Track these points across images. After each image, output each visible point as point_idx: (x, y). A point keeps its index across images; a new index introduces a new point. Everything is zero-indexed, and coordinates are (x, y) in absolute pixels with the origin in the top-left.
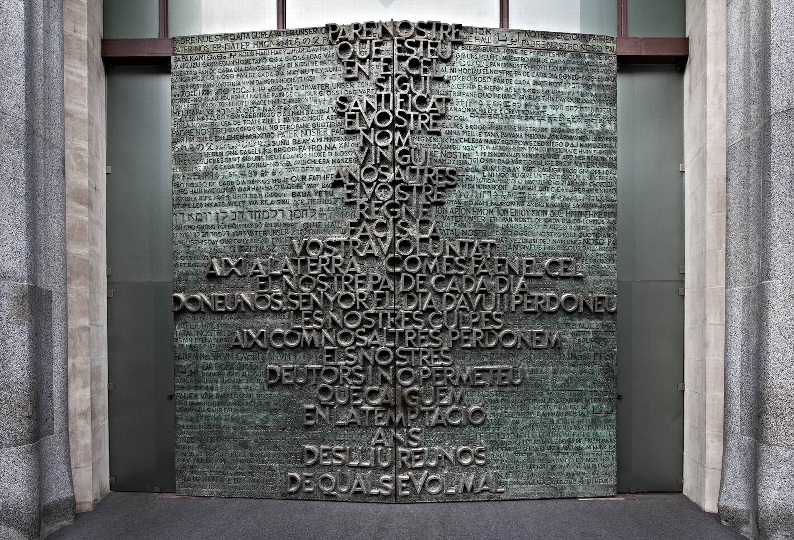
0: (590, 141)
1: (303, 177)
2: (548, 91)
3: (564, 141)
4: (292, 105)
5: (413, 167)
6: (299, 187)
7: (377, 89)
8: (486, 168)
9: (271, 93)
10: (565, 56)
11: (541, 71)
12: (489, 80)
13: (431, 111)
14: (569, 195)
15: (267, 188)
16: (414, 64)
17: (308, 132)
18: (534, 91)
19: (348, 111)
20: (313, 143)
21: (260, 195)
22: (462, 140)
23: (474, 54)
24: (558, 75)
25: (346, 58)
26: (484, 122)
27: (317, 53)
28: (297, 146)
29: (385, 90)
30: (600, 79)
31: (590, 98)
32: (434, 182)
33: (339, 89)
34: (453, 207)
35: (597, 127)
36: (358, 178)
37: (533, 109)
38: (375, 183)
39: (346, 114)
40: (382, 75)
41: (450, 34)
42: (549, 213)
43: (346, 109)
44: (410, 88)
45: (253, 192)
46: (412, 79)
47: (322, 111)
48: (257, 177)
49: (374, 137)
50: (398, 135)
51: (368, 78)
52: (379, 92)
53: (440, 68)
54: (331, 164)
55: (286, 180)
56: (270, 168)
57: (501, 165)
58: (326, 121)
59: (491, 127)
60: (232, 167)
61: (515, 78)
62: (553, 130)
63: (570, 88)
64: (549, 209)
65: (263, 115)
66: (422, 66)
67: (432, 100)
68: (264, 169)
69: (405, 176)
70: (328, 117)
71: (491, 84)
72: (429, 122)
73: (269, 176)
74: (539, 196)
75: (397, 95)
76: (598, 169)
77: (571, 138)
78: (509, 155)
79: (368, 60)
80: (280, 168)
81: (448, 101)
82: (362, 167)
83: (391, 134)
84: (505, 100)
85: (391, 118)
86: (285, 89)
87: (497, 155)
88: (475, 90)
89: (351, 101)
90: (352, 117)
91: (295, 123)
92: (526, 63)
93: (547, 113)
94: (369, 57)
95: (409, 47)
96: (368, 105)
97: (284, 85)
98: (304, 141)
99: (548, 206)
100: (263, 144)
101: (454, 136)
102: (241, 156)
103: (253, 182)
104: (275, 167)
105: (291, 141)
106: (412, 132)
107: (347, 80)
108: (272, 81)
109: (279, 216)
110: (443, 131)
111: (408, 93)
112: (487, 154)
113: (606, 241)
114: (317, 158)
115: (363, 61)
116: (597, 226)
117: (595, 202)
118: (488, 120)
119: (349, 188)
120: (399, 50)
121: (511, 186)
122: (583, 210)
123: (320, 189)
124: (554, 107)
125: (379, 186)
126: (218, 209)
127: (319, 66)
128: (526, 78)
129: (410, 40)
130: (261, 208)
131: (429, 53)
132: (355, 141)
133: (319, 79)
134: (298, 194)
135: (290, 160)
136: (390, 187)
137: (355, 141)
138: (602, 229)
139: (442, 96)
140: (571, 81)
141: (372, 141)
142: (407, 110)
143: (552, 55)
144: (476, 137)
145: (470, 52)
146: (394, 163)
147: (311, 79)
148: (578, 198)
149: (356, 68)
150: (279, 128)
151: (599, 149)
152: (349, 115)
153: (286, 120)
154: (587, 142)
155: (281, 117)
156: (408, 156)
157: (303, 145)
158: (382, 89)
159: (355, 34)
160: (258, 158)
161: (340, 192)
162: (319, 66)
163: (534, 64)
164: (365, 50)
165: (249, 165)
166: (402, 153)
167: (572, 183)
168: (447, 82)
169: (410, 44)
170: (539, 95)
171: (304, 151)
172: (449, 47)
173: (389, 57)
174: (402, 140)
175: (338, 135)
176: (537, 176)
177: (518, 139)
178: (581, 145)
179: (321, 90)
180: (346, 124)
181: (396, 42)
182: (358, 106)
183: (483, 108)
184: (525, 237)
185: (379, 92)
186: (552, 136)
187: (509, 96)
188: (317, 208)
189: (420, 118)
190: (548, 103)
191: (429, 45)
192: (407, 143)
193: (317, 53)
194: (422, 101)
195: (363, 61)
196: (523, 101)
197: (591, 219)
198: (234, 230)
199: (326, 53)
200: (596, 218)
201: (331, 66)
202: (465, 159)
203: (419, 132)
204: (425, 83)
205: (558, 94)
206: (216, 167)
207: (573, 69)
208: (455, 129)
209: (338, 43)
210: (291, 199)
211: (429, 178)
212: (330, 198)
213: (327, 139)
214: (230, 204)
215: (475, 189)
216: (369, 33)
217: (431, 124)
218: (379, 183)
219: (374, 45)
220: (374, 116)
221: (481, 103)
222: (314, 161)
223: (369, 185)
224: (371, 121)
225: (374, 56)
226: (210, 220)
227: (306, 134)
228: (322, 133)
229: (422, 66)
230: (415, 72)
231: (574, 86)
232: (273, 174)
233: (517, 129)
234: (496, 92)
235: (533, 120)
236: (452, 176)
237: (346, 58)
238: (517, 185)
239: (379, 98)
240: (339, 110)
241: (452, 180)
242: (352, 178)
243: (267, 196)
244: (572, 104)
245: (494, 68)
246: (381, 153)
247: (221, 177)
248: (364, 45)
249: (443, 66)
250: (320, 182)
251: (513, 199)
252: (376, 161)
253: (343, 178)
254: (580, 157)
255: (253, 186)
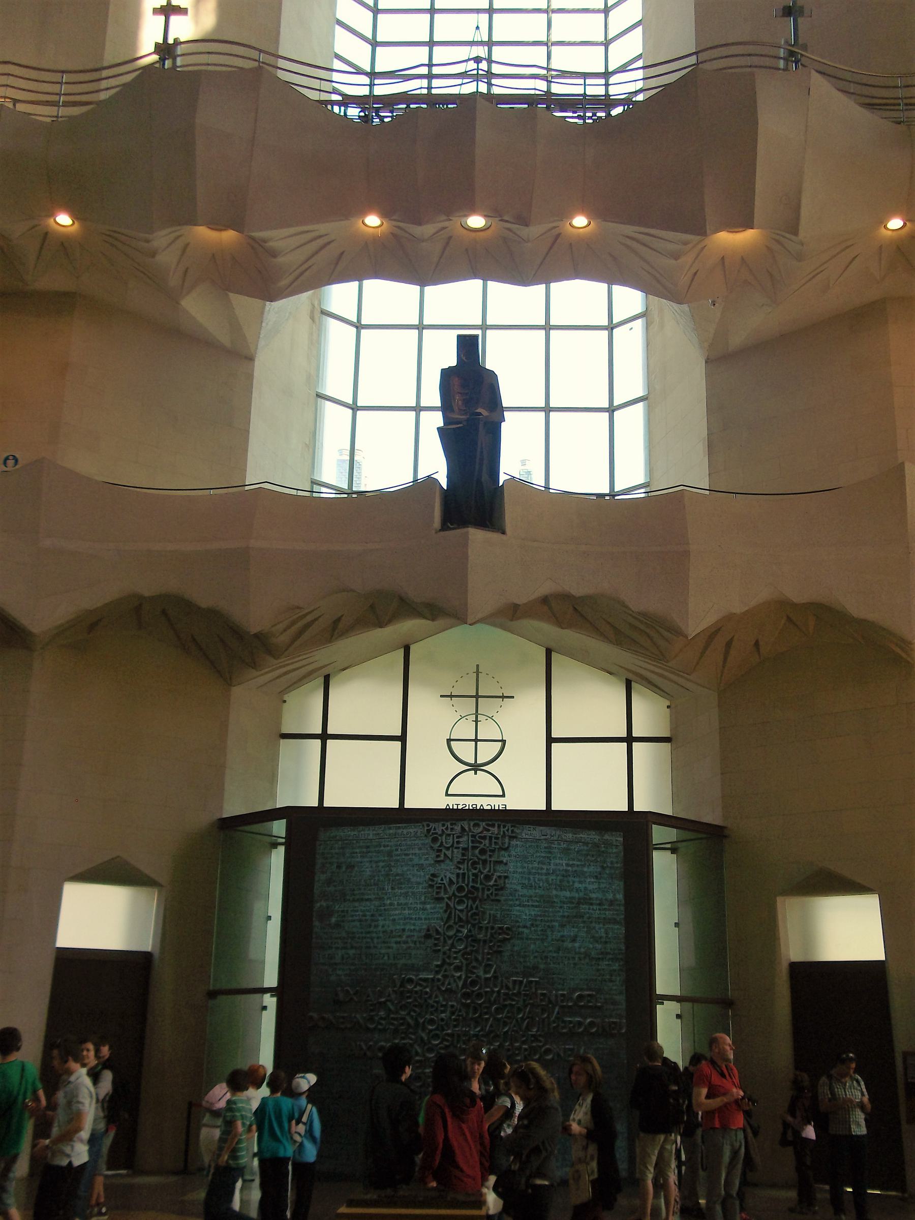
0: (606, 907)
1: (404, 930)
2: (576, 871)
3: (587, 907)
4: (397, 878)
5: (481, 925)
6: (400, 936)
7: (457, 869)
8: (532, 925)
9: (383, 870)
10: (587, 846)
11: (571, 856)
12: (535, 863)
13: (494, 885)
14: (591, 946)
15: (378, 938)
16: (483, 852)
17: (408, 898)
18: (566, 871)
19: (436, 884)
20: (411, 906)
21: (373, 943)
22: (515, 905)
23: (524, 845)
24: (583, 860)
25: (436, 846)
26: (531, 892)
27: (416, 842)
28: (400, 907)
29: (462, 870)
30: (612, 863)
31: (605, 876)
32: (495, 936)
33: (430, 868)
34: (509, 954)
35: (610, 896)
36: (442, 934)
37: (565, 883)
38: (454, 936)
39: (435, 886)
40: (461, 859)
41: (508, 830)
42: (577, 959)
43: (435, 882)
44: (480, 869)
45: (369, 940)
46: (481, 863)
47: (419, 883)
48: (372, 929)
49: (454, 903)
50: (470, 902)
51: (451, 860)
52: (458, 871)
53: (501, 855)
54: (423, 921)
55: (392, 931)
56: (381, 923)
57: (543, 924)
58: (421, 890)
59: (536, 897)
60: (354, 921)
61: (552, 861)
62: (579, 899)
63: (592, 869)
64: (577, 956)
65: (378, 885)
66: (489, 853)
67: (495, 877)
68: (376, 923)
69: (475, 932)
70: (422, 888)
71: (536, 865)
72: (492, 892)
73: (380, 928)
74: (570, 945)
75: (470, 873)
76: (611, 926)
77: (592, 904)
78: (549, 916)
79: (451, 849)
80: (387, 922)
81: (506, 877)
82: (444, 925)
83: (466, 902)
84: (546, 877)
85: (466, 890)
86: (393, 866)
87: (540, 916)
88: (525, 870)
89: (439, 876)
90: (439, 888)
91: (399, 891)
92: (560, 851)
93: (575, 886)
94: (452, 846)
95: (479, 840)
96: (450, 879)
97: (393, 864)
98: (406, 904)
99: (576, 953)
100: (376, 905)
101: (511, 902)
102: (361, 913)
103: (369, 933)
104: (384, 922)
105: (396, 903)
106: (480, 900)
107: (436, 861)
108: (383, 861)
109: (386, 958)
110: (503, 898)
111: (478, 872)
112: (533, 915)
113: (618, 979)
114: (414, 917)
115: (448, 849)
116: (611, 968)
117: (609, 950)
118: (534, 891)
119: (436, 939)
120: (473, 842)
121: (550, 939)
122: (600, 956)
123: (415, 939)
124: (580, 882)
125: (457, 938)
126: (343, 951)
127: (417, 851)
128: (561, 862)
129: (480, 835)
130: (373, 951)
131: (493, 843)
132: (441, 905)
133: (416, 860)
134: (399, 943)
135: (395, 917)
136: (464, 939)
137: (441, 905)
138: (615, 971)
139: (502, 874)
140: (592, 864)
141: (452, 905)
142: (477, 884)
143: (578, 845)
144: (525, 903)
145: (522, 843)
146: (468, 922)
147: (411, 860)
148: (597, 948)
149: (443, 853)
150: (388, 894)
151: (612, 912)
152: (436, 887)
153: (393, 888)
154: (604, 907)
155: (390, 887)
156: (477, 917)
157: (405, 906)
158: (460, 869)
159: (442, 829)
160: (372, 915)
161: (430, 942)
162: (417, 851)
163: (566, 851)
164: (450, 841)
165: (366, 920)
166: (475, 914)
167: (593, 937)
168: (506, 864)
169: (479, 837)
170: (570, 873)
171: (405, 912)
172: (507, 840)
173: (466, 846)
174: (473, 905)
175: (429, 901)
176: (569, 931)
177: (556, 905)
178: (599, 910)
179: (417, 868)
180: (435, 894)
181: (470, 836)
182: (443, 881)
183: (530, 882)
184: (560, 976)
185: (458, 871)
186: (579, 903)
187: (549, 874)
188: (414, 952)
189: (486, 890)
190: (577, 879)
191: (493, 839)
192: (477, 908)
193: (416, 842)
194: (488, 878)
195: (448, 849)
196: (559, 878)
197: (607, 963)
198: (353, 968)
199: (422, 842)
200: (610, 963)
201: (426, 851)
202: (517, 919)
203: (485, 900)
204: (490, 865)
205: (583, 873)
206: (343, 921)
207: (593, 856)
208: (510, 897)
209: (431, 836)
210: (394, 945)
211: (491, 933)
212: (422, 946)
213: (421, 903)
214: (352, 947)
215: (524, 941)
216: (452, 829)
217: (494, 894)
218: (457, 936)
219: (455, 838)
220: (454, 887)
221: (529, 879)
222: (411, 919)
223: (450, 937)
224: (452, 892)
225: (455, 845)
226: (338, 959)
227: (407, 899)
228: (418, 899)
229: (489, 853)
230: (484, 857)
231: (593, 867)
232: (383, 926)
233: (554, 898)
234: (540, 871)
235: (565, 892)
236: (507, 931)
237: (436, 846)
238: (554, 937)
239: (458, 875)
240: (430, 883)
241: (508, 934)
242: (438, 932)
243: (378, 943)
244: (593, 880)
245: (539, 854)
246: (458, 915)
247: (346, 928)
248: (449, 838)
249: (503, 852)
250: (415, 934)
251: (551, 949)
252: (455, 920)
253: (431, 932)
254: (599, 918)
255: (368, 935)
